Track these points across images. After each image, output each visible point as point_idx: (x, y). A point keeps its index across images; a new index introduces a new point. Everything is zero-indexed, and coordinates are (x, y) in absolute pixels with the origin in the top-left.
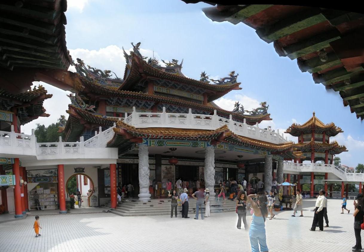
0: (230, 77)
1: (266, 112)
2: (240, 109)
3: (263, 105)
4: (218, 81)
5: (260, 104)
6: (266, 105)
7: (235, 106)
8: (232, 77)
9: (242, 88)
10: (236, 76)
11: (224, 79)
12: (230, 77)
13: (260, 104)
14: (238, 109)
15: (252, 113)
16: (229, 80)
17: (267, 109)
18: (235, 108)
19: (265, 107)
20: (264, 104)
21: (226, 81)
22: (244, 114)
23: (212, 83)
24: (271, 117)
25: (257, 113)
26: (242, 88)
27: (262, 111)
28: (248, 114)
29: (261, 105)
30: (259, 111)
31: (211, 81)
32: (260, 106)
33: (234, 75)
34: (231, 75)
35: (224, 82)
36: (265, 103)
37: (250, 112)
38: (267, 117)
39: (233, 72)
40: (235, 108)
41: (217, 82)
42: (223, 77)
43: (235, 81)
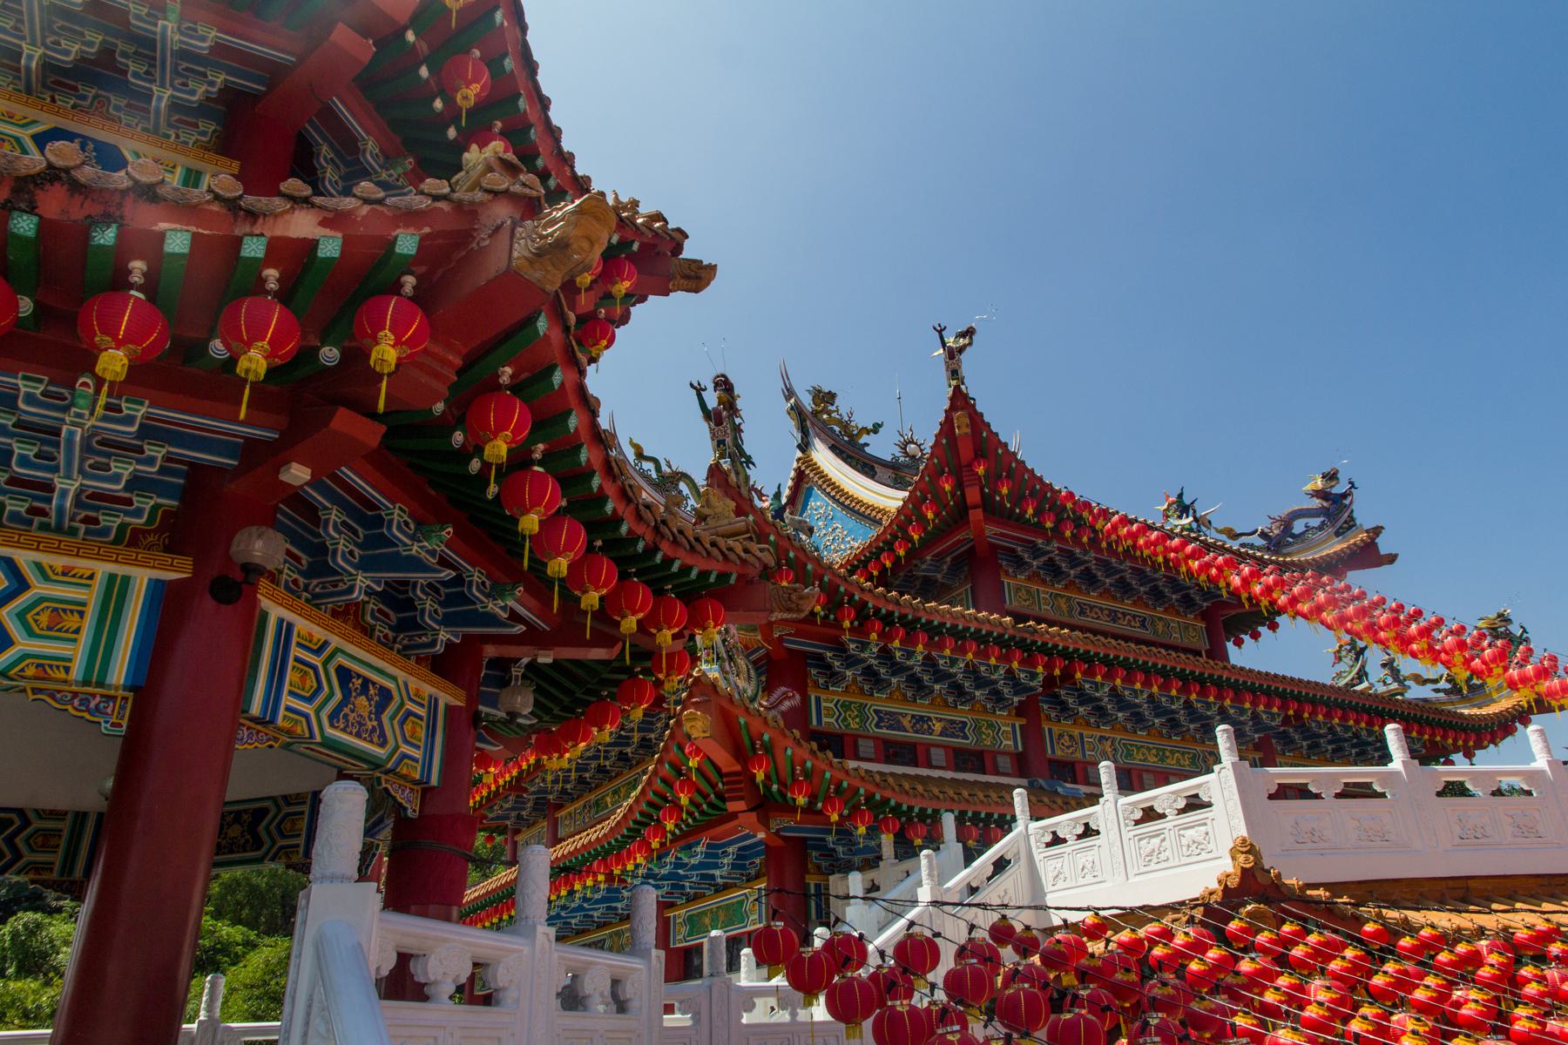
9: (1396, 556)
10: (1345, 496)
11: (1287, 523)
16: (1315, 522)
21: (1298, 526)
26: (1396, 556)
31: (1224, 537)
33: (1339, 489)
35: (1293, 536)
42: (1284, 511)
43: (1351, 524)
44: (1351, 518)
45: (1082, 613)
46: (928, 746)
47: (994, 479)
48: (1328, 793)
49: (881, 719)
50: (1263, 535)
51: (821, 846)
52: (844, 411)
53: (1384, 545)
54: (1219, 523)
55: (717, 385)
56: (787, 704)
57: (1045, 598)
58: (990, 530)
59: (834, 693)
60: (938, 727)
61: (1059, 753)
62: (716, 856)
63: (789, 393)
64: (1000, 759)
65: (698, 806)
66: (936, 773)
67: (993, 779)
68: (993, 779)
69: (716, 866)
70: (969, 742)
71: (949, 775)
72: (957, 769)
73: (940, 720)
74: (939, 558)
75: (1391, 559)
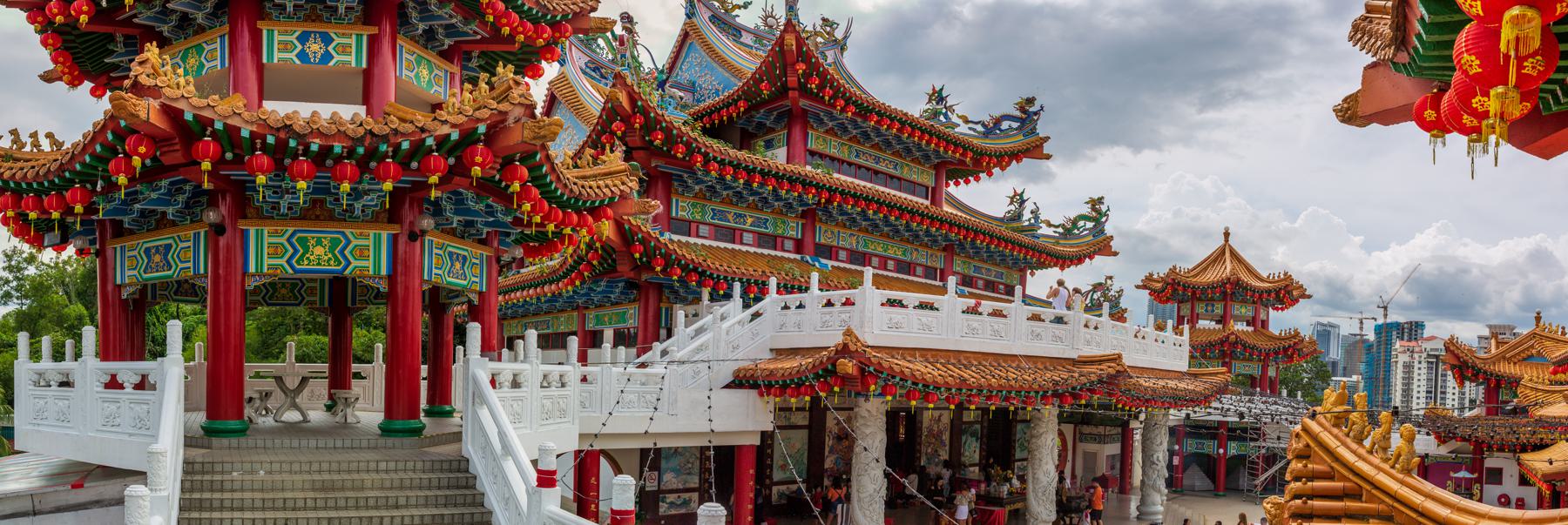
47: (807, 76)
51: (671, 287)
57: (833, 148)
58: (803, 103)
66: (744, 248)
67: (779, 254)
68: (779, 254)
71: (752, 250)
72: (759, 246)
74: (770, 111)
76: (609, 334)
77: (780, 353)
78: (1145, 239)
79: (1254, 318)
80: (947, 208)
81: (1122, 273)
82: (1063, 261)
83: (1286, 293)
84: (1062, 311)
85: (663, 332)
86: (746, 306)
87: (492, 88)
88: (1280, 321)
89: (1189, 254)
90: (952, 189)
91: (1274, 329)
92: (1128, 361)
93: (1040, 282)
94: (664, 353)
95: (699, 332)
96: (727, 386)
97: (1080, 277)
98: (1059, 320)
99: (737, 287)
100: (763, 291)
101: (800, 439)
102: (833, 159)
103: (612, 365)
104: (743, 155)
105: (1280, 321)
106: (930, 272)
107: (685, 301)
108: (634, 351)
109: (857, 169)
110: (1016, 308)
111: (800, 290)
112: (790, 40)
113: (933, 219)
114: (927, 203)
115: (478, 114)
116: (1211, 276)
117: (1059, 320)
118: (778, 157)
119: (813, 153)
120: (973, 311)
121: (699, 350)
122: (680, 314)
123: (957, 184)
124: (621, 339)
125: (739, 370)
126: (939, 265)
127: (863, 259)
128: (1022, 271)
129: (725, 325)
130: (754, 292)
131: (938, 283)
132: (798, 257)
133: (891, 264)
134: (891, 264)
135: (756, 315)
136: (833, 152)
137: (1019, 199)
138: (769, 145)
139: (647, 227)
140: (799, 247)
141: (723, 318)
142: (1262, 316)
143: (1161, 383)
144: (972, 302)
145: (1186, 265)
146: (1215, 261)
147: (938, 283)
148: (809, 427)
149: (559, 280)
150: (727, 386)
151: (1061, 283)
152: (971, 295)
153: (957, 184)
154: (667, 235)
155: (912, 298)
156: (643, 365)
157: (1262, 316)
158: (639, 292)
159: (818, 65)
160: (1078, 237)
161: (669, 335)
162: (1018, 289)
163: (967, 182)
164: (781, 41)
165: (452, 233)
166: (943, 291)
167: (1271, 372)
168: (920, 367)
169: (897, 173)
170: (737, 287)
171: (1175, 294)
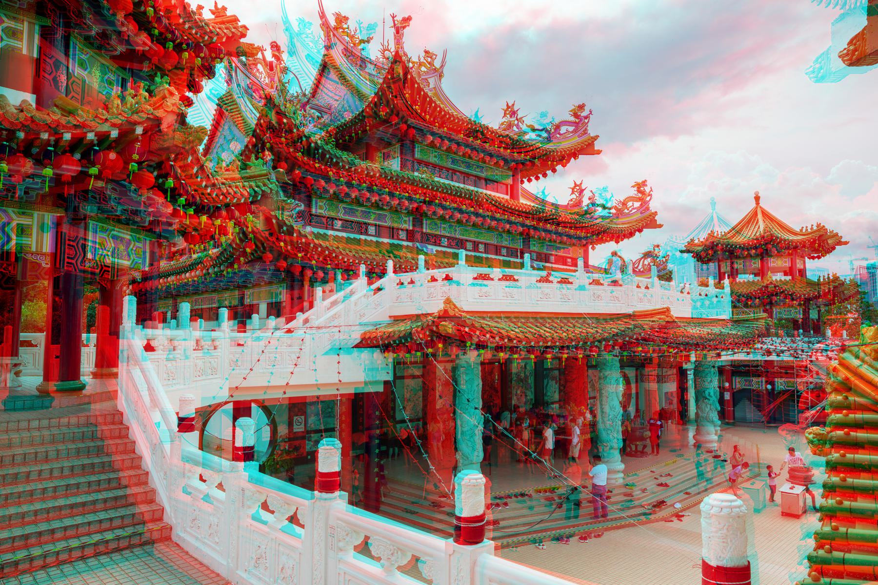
0: (572, 119)
1: (648, 209)
2: (586, 202)
3: (639, 191)
4: (547, 131)
5: (633, 187)
6: (647, 189)
7: (573, 193)
8: (577, 120)
10: (586, 117)
12: (572, 119)
13: (633, 187)
14: (579, 203)
15: (613, 211)
16: (571, 129)
17: (648, 199)
18: (574, 196)
19: (643, 193)
20: (640, 186)
21: (563, 129)
22: (597, 214)
23: (531, 136)
24: (659, 219)
25: (626, 211)
27: (637, 204)
28: (605, 213)
29: (635, 189)
30: (630, 204)
31: (528, 130)
32: (633, 192)
34: (576, 115)
35: (559, 134)
36: (644, 183)
37: (610, 209)
38: (650, 222)
39: (581, 107)
40: (574, 196)
41: (544, 135)
42: (557, 121)
43: (585, 132)
44: (586, 129)
45: (453, 163)
46: (367, 224)
48: (496, 279)
49: (345, 212)
50: (547, 131)
52: (352, 28)
53: (597, 146)
54: (528, 121)
55: (272, 47)
56: (298, 209)
59: (324, 198)
60: (373, 216)
61: (429, 231)
62: (265, 270)
63: (323, 15)
64: (400, 232)
65: (256, 251)
66: (369, 238)
67: (396, 242)
69: (265, 274)
70: (388, 224)
73: (374, 213)
75: (599, 152)
76: (263, 308)
77: (397, 319)
78: (688, 211)
79: (791, 268)
80: (523, 201)
81: (668, 239)
82: (618, 236)
83: (821, 243)
84: (618, 276)
85: (306, 304)
86: (370, 283)
87: (151, 96)
88: (817, 268)
89: (725, 219)
90: (526, 185)
91: (812, 275)
92: (675, 313)
93: (600, 254)
94: (306, 321)
95: (334, 304)
96: (357, 346)
97: (631, 249)
98: (615, 283)
99: (363, 268)
100: (384, 272)
101: (414, 384)
102: (435, 166)
103: (265, 331)
104: (364, 164)
105: (817, 268)
106: (512, 252)
107: (325, 281)
108: (282, 320)
109: (452, 173)
110: (580, 276)
111: (412, 270)
112: (399, 70)
113: (512, 212)
114: (507, 197)
115: (135, 117)
116: (747, 236)
117: (615, 283)
118: (394, 165)
119: (420, 162)
120: (545, 280)
121: (334, 317)
122: (319, 291)
123: (529, 180)
124: (275, 310)
125: (365, 333)
126: (519, 245)
127: (461, 244)
128: (585, 246)
129: (354, 298)
130: (376, 273)
131: (519, 260)
132: (410, 244)
133: (481, 247)
134: (481, 247)
135: (379, 289)
136: (433, 159)
137: (578, 189)
138: (386, 157)
139: (291, 222)
140: (411, 236)
141: (352, 293)
142: (799, 265)
143: (706, 330)
144: (544, 273)
145: (721, 230)
146: (748, 222)
147: (519, 260)
148: (423, 376)
149: (221, 264)
150: (357, 346)
151: (614, 254)
152: (544, 268)
153: (529, 180)
154: (309, 229)
155: (496, 272)
156: (289, 331)
157: (799, 265)
158: (284, 275)
159: (420, 89)
160: (628, 215)
161: (311, 306)
162: (580, 262)
163: (537, 178)
164: (391, 70)
165: (118, 220)
166: (522, 266)
167: (813, 315)
168: (504, 326)
169: (483, 175)
170: (363, 268)
171: (716, 254)
